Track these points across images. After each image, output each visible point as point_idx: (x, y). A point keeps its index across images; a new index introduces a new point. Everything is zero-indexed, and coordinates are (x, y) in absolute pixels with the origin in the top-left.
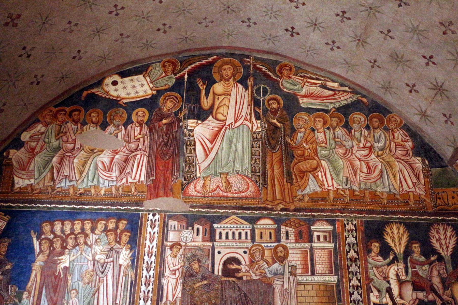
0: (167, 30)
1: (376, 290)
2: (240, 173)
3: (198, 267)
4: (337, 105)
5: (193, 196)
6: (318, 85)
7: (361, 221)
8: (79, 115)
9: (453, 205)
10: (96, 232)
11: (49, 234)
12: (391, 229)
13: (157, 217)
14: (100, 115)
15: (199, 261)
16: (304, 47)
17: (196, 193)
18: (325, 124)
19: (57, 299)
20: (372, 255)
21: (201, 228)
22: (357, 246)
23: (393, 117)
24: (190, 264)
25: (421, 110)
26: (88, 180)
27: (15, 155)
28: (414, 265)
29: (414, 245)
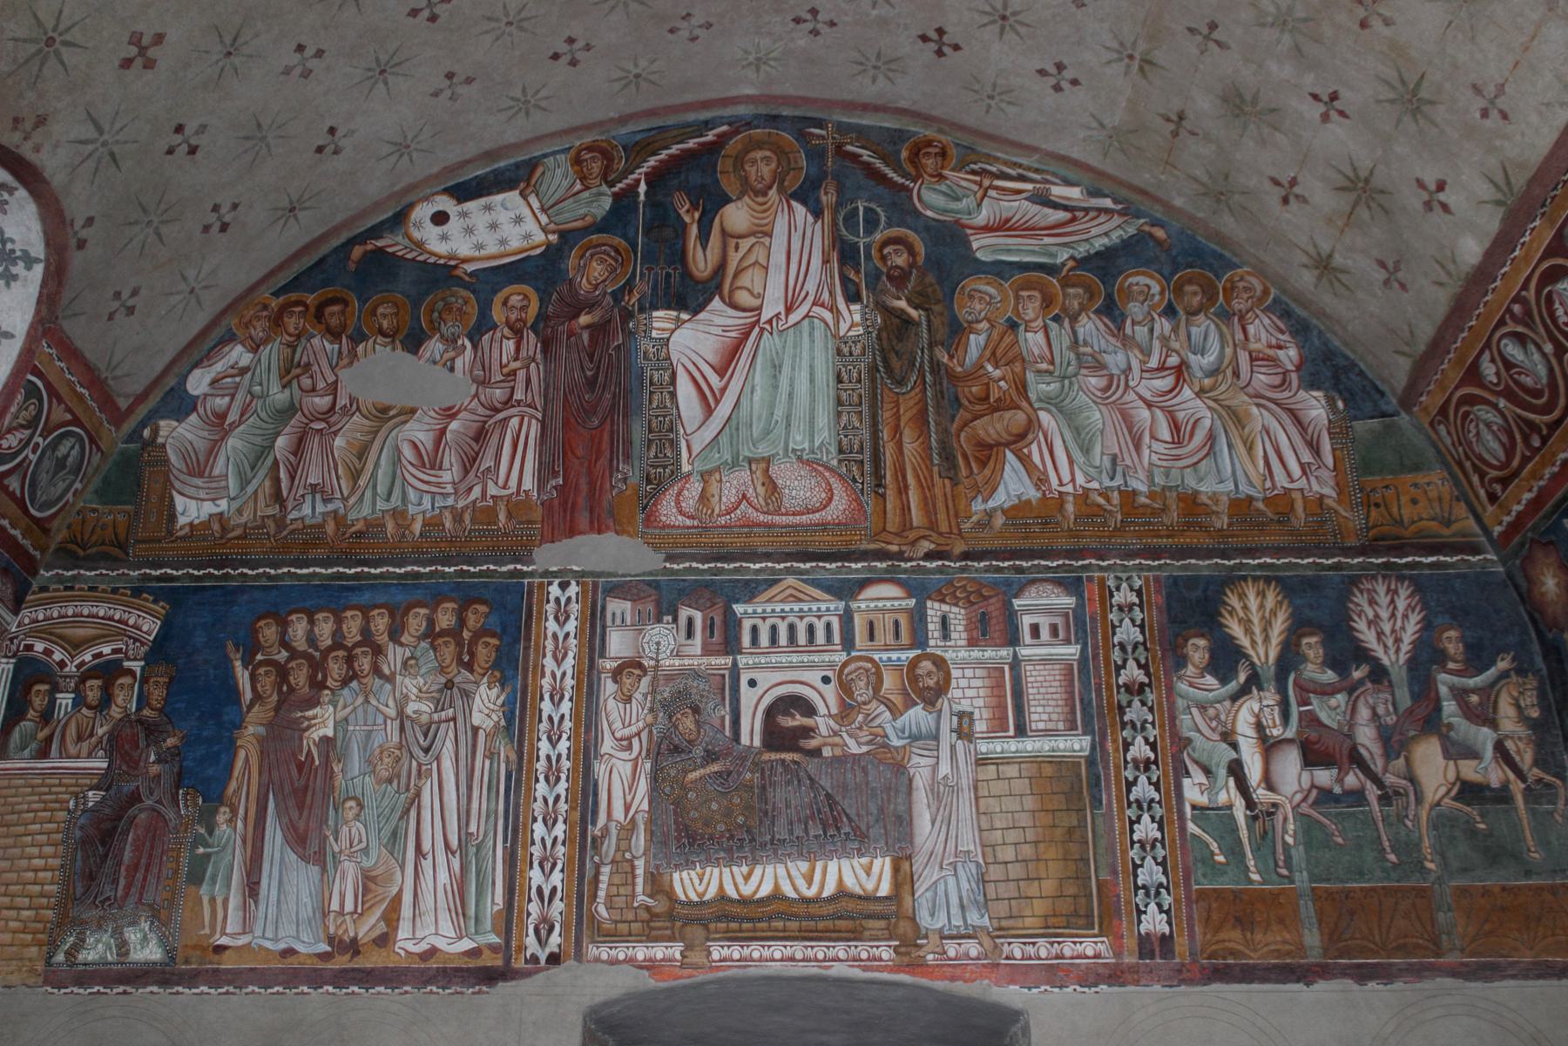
0: (579, 55)
1: (1200, 771)
2: (805, 457)
3: (692, 727)
4: (1082, 250)
5: (674, 526)
6: (1024, 195)
7: (1157, 579)
8: (343, 312)
9: (1413, 522)
10: (403, 640)
11: (275, 650)
12: (1242, 596)
13: (573, 589)
14: (402, 312)
15: (696, 710)
16: (977, 87)
17: (680, 518)
18: (1047, 307)
20: (1188, 673)
21: (698, 617)
22: (1146, 649)
23: (1242, 279)
24: (670, 717)
25: (1319, 254)
26: (375, 494)
27: (174, 434)
28: (1304, 694)
29: (1305, 641)
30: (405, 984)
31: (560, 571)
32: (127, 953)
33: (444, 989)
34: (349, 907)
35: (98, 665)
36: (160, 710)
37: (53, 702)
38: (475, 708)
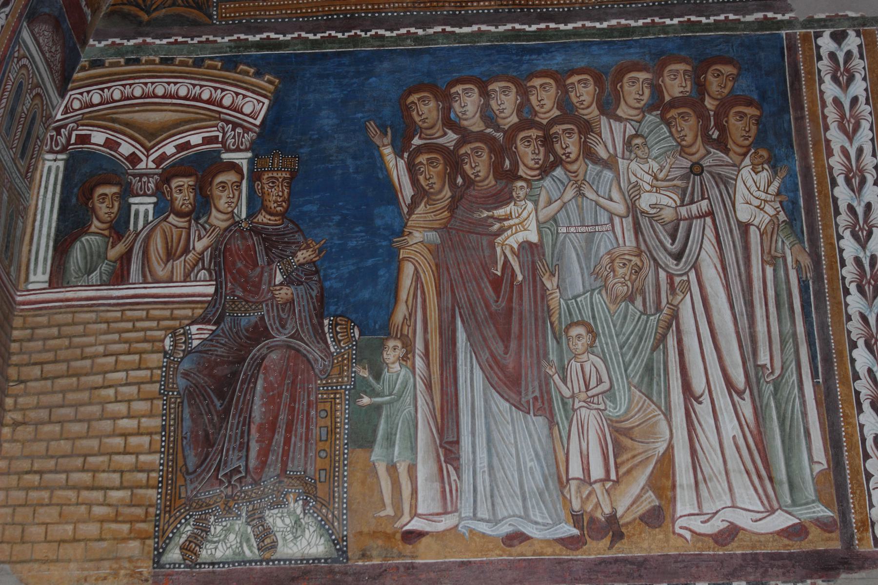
10: (619, 112)
13: (853, 42)
19: (519, 365)
31: (829, 19)
32: (274, 546)
34: (597, 472)
35: (188, 157)
36: (283, 215)
38: (739, 199)
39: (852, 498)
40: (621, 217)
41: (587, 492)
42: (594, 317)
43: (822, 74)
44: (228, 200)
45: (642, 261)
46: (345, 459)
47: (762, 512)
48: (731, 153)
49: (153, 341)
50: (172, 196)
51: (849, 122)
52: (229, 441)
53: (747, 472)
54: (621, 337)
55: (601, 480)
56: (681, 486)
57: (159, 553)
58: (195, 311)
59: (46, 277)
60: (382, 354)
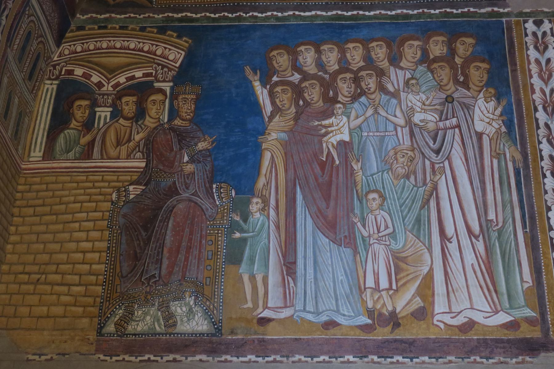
10: (402, 64)
13: (547, 26)
19: (336, 216)
30: (449, 354)
32: (175, 325)
33: (487, 358)
34: (384, 283)
37: (93, 114)
38: (476, 118)
39: (549, 305)
40: (402, 127)
41: (377, 297)
42: (384, 188)
43: (528, 44)
44: (157, 111)
45: (414, 154)
46: (223, 271)
47: (490, 312)
48: (471, 90)
49: (105, 195)
50: (122, 108)
51: (545, 73)
52: (150, 258)
53: (481, 287)
54: (400, 200)
55: (386, 289)
56: (438, 294)
57: (101, 326)
58: (133, 177)
59: (41, 154)
60: (249, 206)
